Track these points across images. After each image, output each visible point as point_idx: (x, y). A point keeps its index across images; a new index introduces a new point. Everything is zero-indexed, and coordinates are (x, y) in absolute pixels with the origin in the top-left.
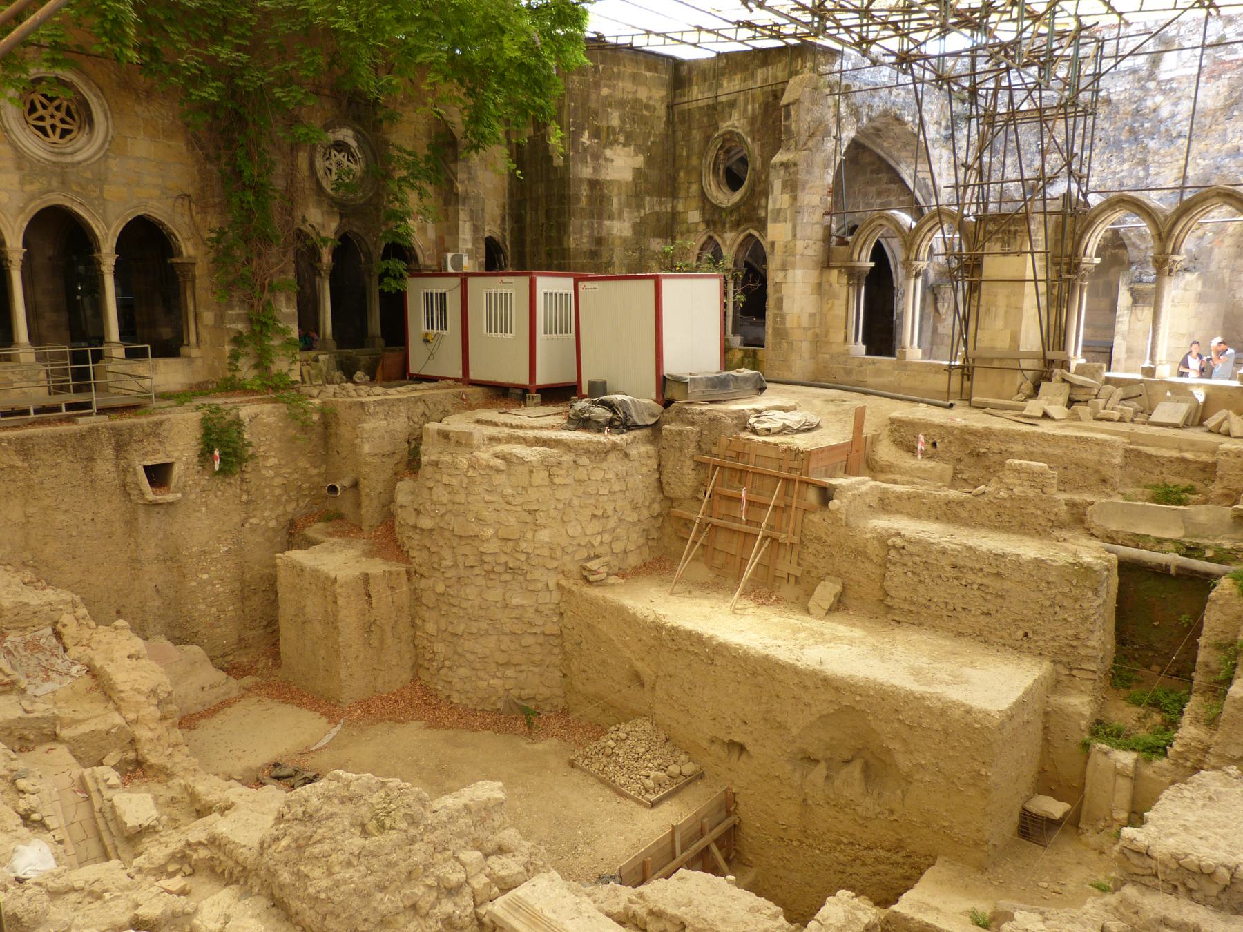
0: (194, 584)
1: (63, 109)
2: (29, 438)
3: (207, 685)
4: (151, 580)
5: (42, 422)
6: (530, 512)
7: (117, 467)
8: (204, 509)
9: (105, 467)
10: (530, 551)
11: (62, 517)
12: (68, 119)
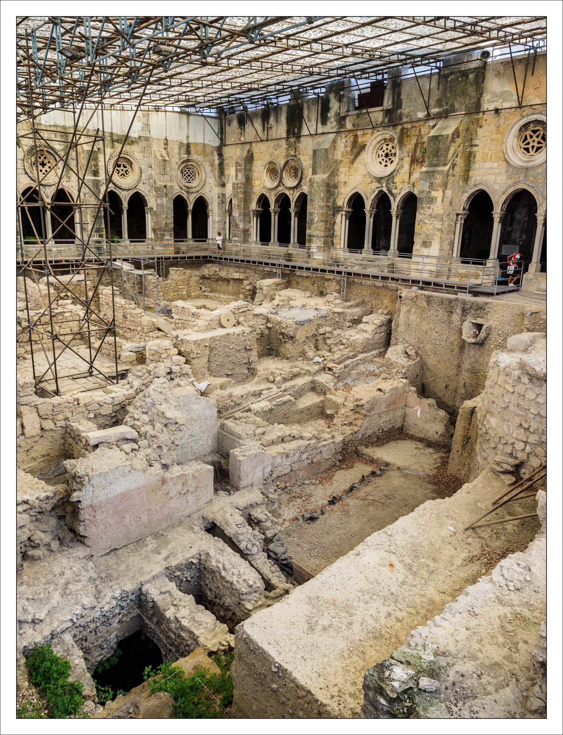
4: (463, 379)
7: (461, 319)
9: (456, 318)
11: (435, 334)
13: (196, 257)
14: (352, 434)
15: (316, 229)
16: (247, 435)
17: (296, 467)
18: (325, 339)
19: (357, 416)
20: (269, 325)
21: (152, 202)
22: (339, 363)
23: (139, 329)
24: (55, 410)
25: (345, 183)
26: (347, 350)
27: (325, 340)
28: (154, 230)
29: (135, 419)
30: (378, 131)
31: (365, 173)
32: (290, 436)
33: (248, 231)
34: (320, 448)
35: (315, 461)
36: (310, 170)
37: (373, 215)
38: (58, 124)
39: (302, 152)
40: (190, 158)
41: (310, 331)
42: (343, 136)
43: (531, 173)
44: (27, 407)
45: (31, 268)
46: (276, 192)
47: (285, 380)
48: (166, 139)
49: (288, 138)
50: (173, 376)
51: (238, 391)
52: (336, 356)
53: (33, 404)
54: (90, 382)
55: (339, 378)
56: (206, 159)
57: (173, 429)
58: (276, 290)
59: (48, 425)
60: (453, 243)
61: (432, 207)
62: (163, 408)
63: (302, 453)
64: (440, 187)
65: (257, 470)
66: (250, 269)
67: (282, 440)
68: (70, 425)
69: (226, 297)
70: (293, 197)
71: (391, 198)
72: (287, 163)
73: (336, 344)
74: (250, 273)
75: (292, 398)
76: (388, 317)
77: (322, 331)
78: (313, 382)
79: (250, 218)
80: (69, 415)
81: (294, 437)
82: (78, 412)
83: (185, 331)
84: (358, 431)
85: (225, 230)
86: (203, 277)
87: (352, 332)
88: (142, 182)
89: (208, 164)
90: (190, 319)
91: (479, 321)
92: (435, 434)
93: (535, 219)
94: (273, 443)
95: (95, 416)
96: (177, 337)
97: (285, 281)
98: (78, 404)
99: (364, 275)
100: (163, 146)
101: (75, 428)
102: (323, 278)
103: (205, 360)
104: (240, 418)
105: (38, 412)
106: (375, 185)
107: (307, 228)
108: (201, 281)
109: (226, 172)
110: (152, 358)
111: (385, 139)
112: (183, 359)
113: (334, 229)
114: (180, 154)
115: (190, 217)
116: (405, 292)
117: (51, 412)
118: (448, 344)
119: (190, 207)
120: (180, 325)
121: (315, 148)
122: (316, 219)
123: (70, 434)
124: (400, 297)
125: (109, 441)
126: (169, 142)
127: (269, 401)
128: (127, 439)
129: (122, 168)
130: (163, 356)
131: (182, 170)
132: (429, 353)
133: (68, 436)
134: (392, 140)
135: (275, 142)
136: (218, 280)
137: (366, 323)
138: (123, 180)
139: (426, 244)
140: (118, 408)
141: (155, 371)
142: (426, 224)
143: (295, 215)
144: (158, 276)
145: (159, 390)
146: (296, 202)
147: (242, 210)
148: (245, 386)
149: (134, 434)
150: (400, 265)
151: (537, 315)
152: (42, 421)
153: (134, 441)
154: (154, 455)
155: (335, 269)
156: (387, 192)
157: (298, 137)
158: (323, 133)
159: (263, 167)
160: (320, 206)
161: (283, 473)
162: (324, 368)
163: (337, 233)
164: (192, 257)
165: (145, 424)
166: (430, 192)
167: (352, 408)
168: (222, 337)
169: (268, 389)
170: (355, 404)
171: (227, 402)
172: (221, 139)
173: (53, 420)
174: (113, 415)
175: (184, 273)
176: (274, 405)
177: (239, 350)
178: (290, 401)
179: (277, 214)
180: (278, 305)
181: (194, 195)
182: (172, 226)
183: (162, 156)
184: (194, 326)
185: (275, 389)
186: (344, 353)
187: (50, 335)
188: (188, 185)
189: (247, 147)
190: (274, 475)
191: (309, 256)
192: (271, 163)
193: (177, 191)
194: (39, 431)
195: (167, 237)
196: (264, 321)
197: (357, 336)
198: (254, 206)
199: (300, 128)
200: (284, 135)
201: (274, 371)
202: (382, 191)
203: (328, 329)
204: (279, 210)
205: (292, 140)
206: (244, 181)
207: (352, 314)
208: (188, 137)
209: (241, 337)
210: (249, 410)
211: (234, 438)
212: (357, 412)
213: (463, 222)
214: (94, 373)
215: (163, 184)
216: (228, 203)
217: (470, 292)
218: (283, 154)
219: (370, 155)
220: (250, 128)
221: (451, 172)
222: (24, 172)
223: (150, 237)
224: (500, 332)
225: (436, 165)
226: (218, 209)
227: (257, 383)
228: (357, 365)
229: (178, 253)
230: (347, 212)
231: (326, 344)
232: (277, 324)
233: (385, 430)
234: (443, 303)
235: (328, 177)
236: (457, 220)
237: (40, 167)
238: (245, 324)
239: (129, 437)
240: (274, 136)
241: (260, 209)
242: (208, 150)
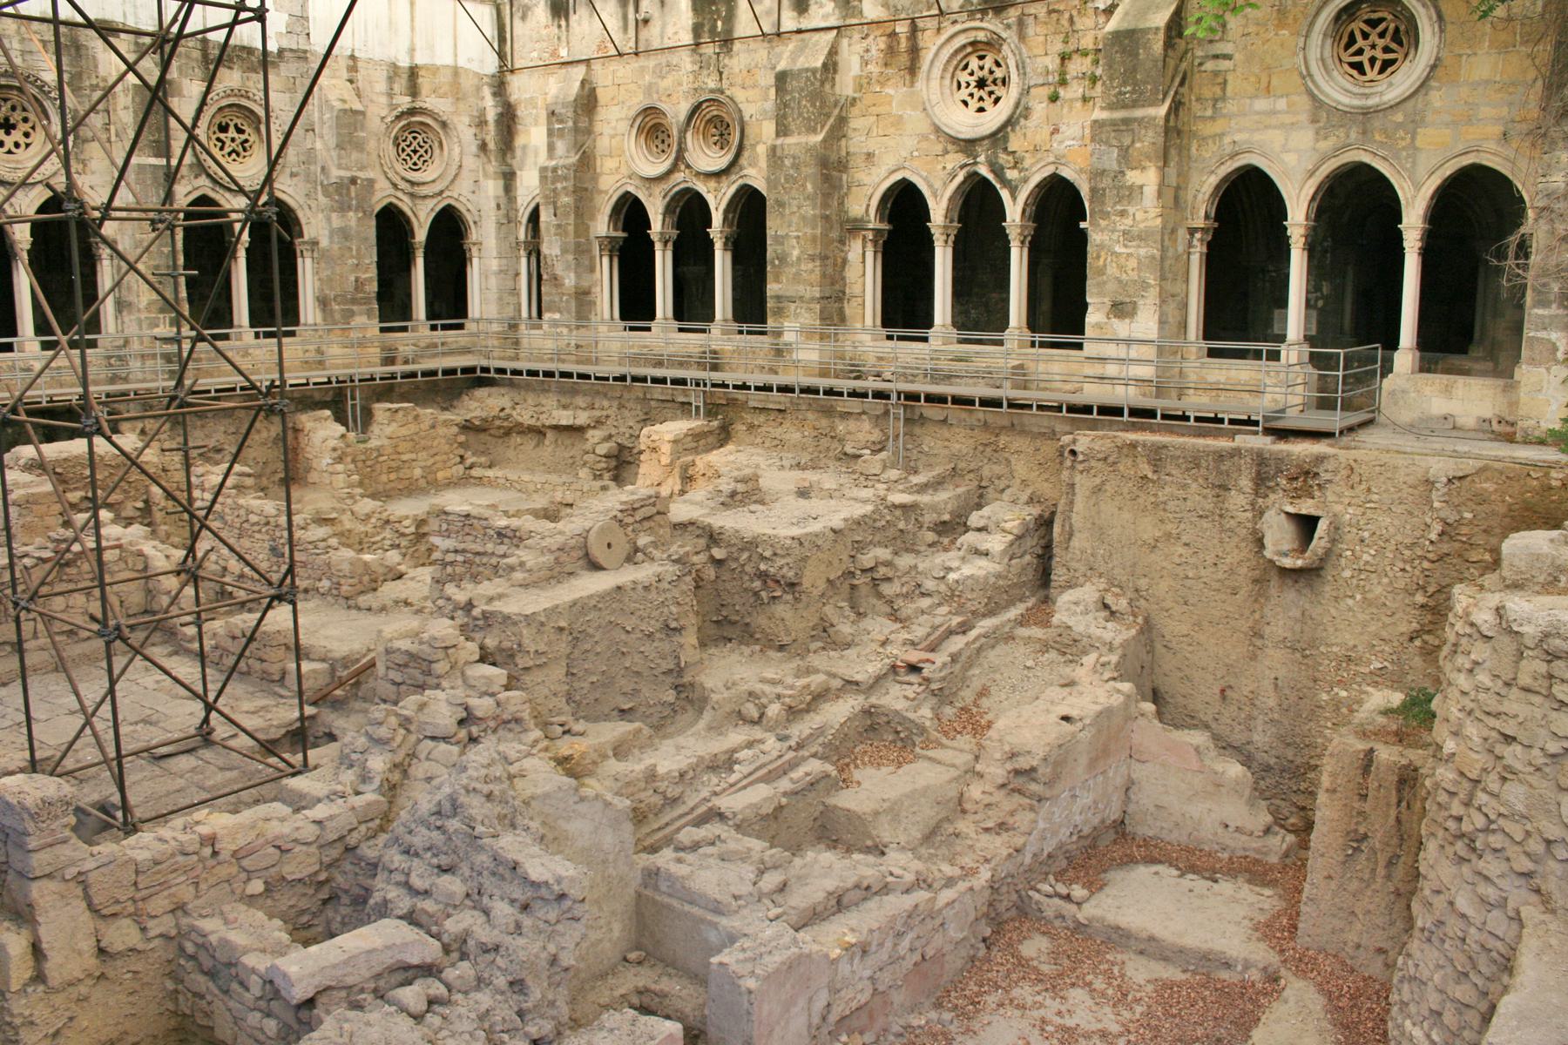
0: (1325, 697)
1: (1389, 35)
2: (1165, 447)
3: (1232, 825)
5: (1170, 431)
6: (1509, 739)
8: (1358, 597)
9: (1238, 501)
10: (1493, 817)
11: (1181, 550)
12: (1394, 46)
13: (447, 372)
14: (1010, 855)
15: (797, 278)
16: (736, 897)
17: (885, 978)
18: (875, 583)
19: (1017, 798)
20: (718, 553)
21: (316, 225)
22: (932, 649)
23: (325, 584)
24: (143, 881)
25: (869, 156)
26: (944, 609)
27: (876, 585)
28: (323, 302)
29: (414, 892)
30: (955, 22)
31: (925, 127)
32: (857, 886)
33: (587, 293)
34: (940, 911)
35: (930, 952)
36: (769, 128)
37: (952, 238)
39: (739, 81)
40: (418, 104)
41: (836, 562)
42: (857, 36)
43: (1377, 123)
44: (52, 885)
45: (24, 417)
46: (665, 186)
47: (793, 713)
49: (697, 44)
50: (475, 730)
51: (668, 758)
52: (919, 632)
53: (70, 872)
54: (209, 769)
55: (942, 696)
56: (461, 105)
57: (552, 916)
58: (696, 451)
59: (122, 935)
60: (1186, 305)
61: (1131, 210)
62: (510, 844)
63: (900, 935)
64: (1149, 158)
65: (795, 1010)
66: (605, 395)
67: (839, 902)
68: (193, 929)
69: (539, 478)
70: (718, 200)
71: (1005, 194)
72: (696, 109)
73: (906, 596)
74: (607, 407)
75: (830, 768)
76: (1035, 511)
77: (867, 560)
78: (867, 712)
79: (592, 259)
80: (186, 893)
81: (868, 888)
82: (212, 881)
83: (487, 588)
84: (1024, 845)
85: (518, 295)
86: (467, 427)
87: (940, 558)
88: (288, 171)
89: (466, 120)
90: (490, 547)
91: (1306, 507)
92: (1220, 830)
93: (1398, 238)
94: (812, 917)
95: (269, 889)
96: (469, 606)
97: (715, 423)
98: (215, 853)
99: (959, 401)
100: (345, 75)
101: (213, 939)
102: (828, 412)
103: (559, 672)
104: (695, 846)
105: (88, 898)
106: (955, 159)
107: (770, 277)
108: (462, 438)
109: (519, 141)
110: (393, 675)
111: (973, 44)
112: (498, 674)
113: (843, 279)
114: (390, 95)
115: (420, 262)
116: (1084, 441)
117: (131, 892)
118: (1221, 575)
119: (421, 235)
120: (459, 570)
121: (779, 68)
122: (796, 253)
123: (192, 957)
124: (1073, 453)
125: (350, 981)
126: (360, 64)
127: (768, 778)
128: (407, 968)
129: (232, 133)
130: (441, 667)
131: (396, 138)
132: (1168, 604)
133: (189, 965)
134: (994, 44)
135: (662, 59)
136: (508, 433)
137: (979, 530)
139: (1121, 309)
140: (335, 852)
141: (422, 718)
142: (1118, 255)
143: (725, 244)
144: (342, 429)
145: (486, 789)
146: (726, 212)
147: (571, 238)
148: (681, 740)
149: (425, 949)
150: (1042, 367)
151: (1466, 482)
152: (101, 924)
153: (428, 970)
154: (504, 1012)
155: (858, 385)
156: (990, 177)
157: (727, 42)
158: (799, 32)
159: (627, 123)
160: (804, 218)
161: (854, 1005)
162: (894, 668)
163: (853, 289)
164: (433, 373)
165: (451, 907)
166: (1122, 173)
167: (1000, 781)
168: (602, 596)
169: (750, 745)
170: (1009, 766)
171: (642, 795)
172: (501, 55)
173: (136, 917)
174: (322, 877)
176: (785, 794)
177: (650, 635)
178: (828, 776)
179: (670, 246)
180: (733, 494)
181: (430, 203)
182: (373, 287)
183: (344, 101)
184: (512, 568)
185: (771, 743)
186: (938, 621)
187: (96, 627)
189: (579, 72)
190: (833, 1017)
191: (779, 352)
192: (649, 111)
193: (382, 195)
194: (91, 962)
195: (360, 320)
196: (702, 542)
197: (967, 570)
198: (602, 226)
199: (730, 18)
200: (687, 38)
201: (758, 687)
202: (976, 174)
203: (883, 553)
204: (674, 233)
205: (709, 50)
206: (574, 159)
207: (934, 508)
208: (412, 50)
209: (653, 595)
210: (721, 816)
211: (695, 910)
212: (1013, 790)
213: (1205, 250)
214: (217, 736)
215: (348, 174)
216: (524, 220)
217: (1269, 431)
218: (685, 87)
219: (935, 83)
220: (585, 23)
221: (1172, 123)
223: (310, 321)
224: (1366, 534)
225: (1134, 104)
226: (497, 238)
227: (710, 728)
228: (979, 650)
229: (389, 361)
230: (877, 232)
231: (880, 596)
232: (742, 550)
233: (1086, 830)
234: (1198, 466)
235: (824, 140)
236: (1190, 245)
238: (657, 554)
239: (415, 961)
240: (656, 44)
241: (620, 234)
242: (467, 83)
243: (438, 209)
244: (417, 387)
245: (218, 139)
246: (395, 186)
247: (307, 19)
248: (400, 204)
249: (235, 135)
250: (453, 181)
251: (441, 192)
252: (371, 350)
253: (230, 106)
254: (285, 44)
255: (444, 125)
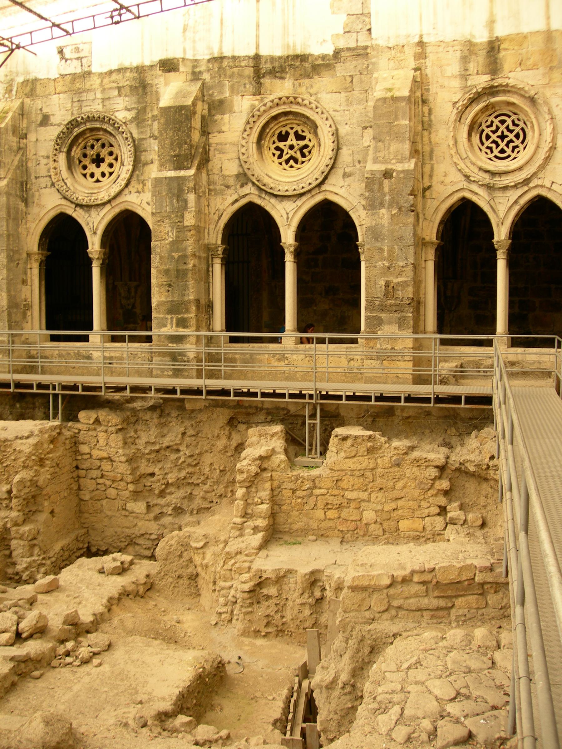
38: (127, 64)
48: (421, 44)
88: (339, 171)
114: (464, 76)
129: (292, 140)
138: (293, 172)
175: (370, 451)
181: (513, 195)
188: (501, 165)
215: (383, 167)
222: (49, 184)
237: (92, 168)
243: (523, 201)
244: (428, 413)
245: (277, 148)
246: (467, 177)
247: (369, 15)
248: (474, 199)
249: (294, 142)
250: (542, 167)
251: (526, 181)
252: (402, 364)
253: (286, 114)
254: (342, 44)
255: (532, 100)
